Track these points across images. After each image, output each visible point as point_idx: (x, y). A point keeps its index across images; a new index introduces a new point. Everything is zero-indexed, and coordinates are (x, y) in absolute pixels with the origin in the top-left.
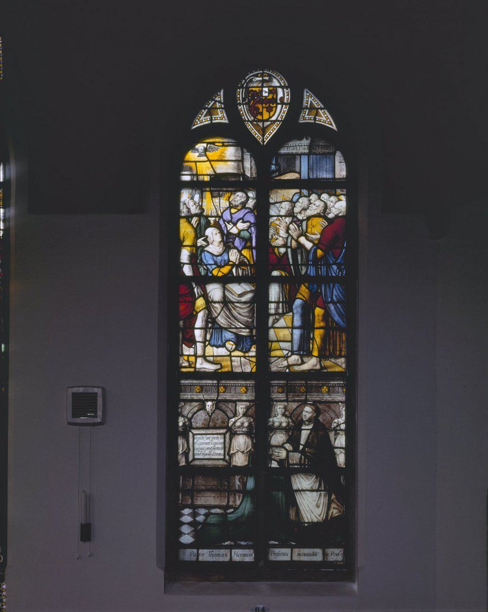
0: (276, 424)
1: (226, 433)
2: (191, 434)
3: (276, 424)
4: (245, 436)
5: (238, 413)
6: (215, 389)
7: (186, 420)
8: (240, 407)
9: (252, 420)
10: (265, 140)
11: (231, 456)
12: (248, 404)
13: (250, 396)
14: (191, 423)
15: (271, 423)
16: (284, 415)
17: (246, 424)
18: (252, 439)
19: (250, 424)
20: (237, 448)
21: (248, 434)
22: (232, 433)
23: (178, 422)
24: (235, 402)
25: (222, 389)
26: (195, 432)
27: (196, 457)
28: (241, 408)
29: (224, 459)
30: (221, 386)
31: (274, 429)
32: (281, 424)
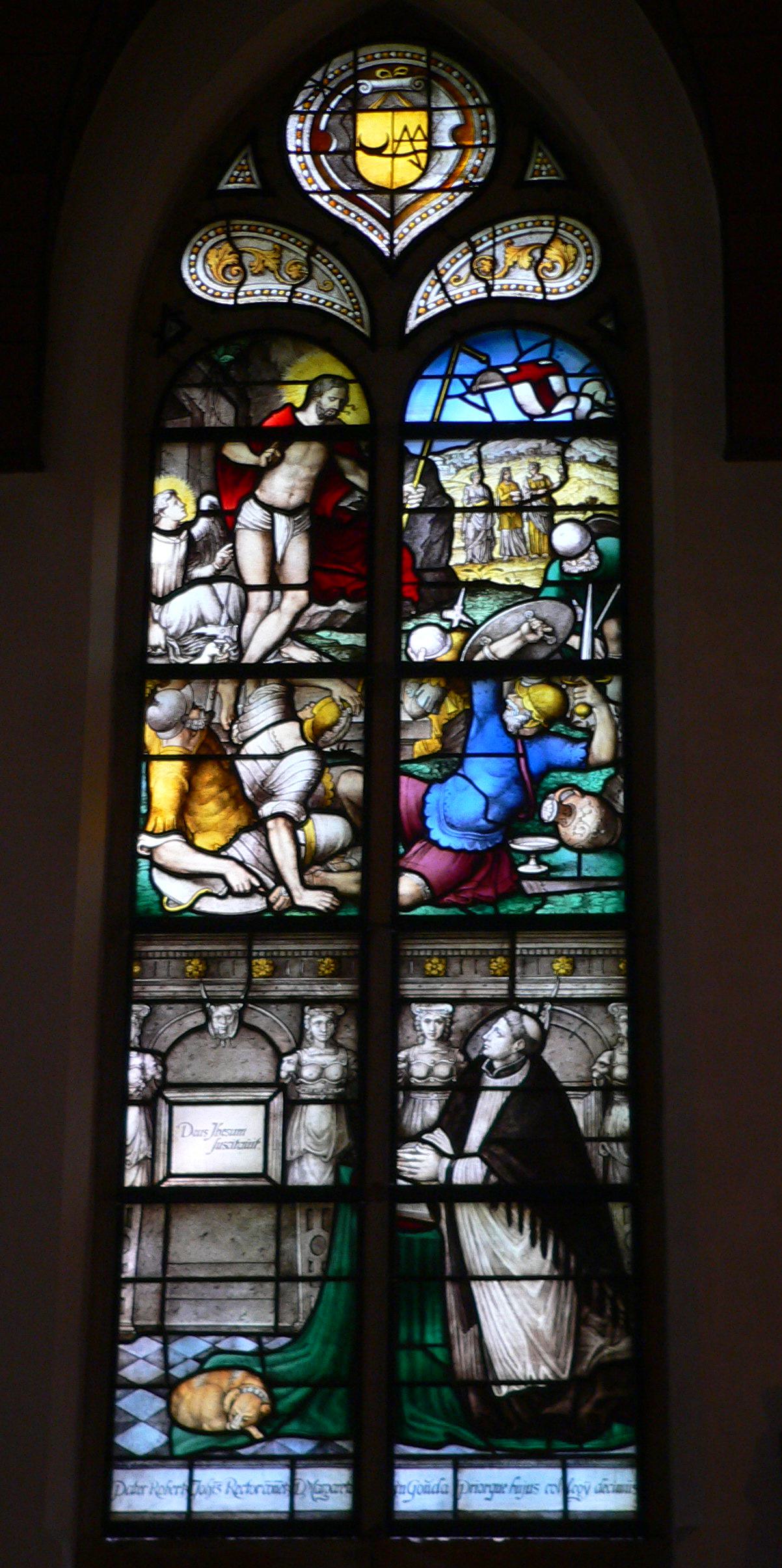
2: (163, 1108)
8: (314, 1020)
10: (396, 241)
11: (286, 1165)
17: (334, 1072)
22: (293, 1105)
28: (319, 1023)
30: (258, 957)
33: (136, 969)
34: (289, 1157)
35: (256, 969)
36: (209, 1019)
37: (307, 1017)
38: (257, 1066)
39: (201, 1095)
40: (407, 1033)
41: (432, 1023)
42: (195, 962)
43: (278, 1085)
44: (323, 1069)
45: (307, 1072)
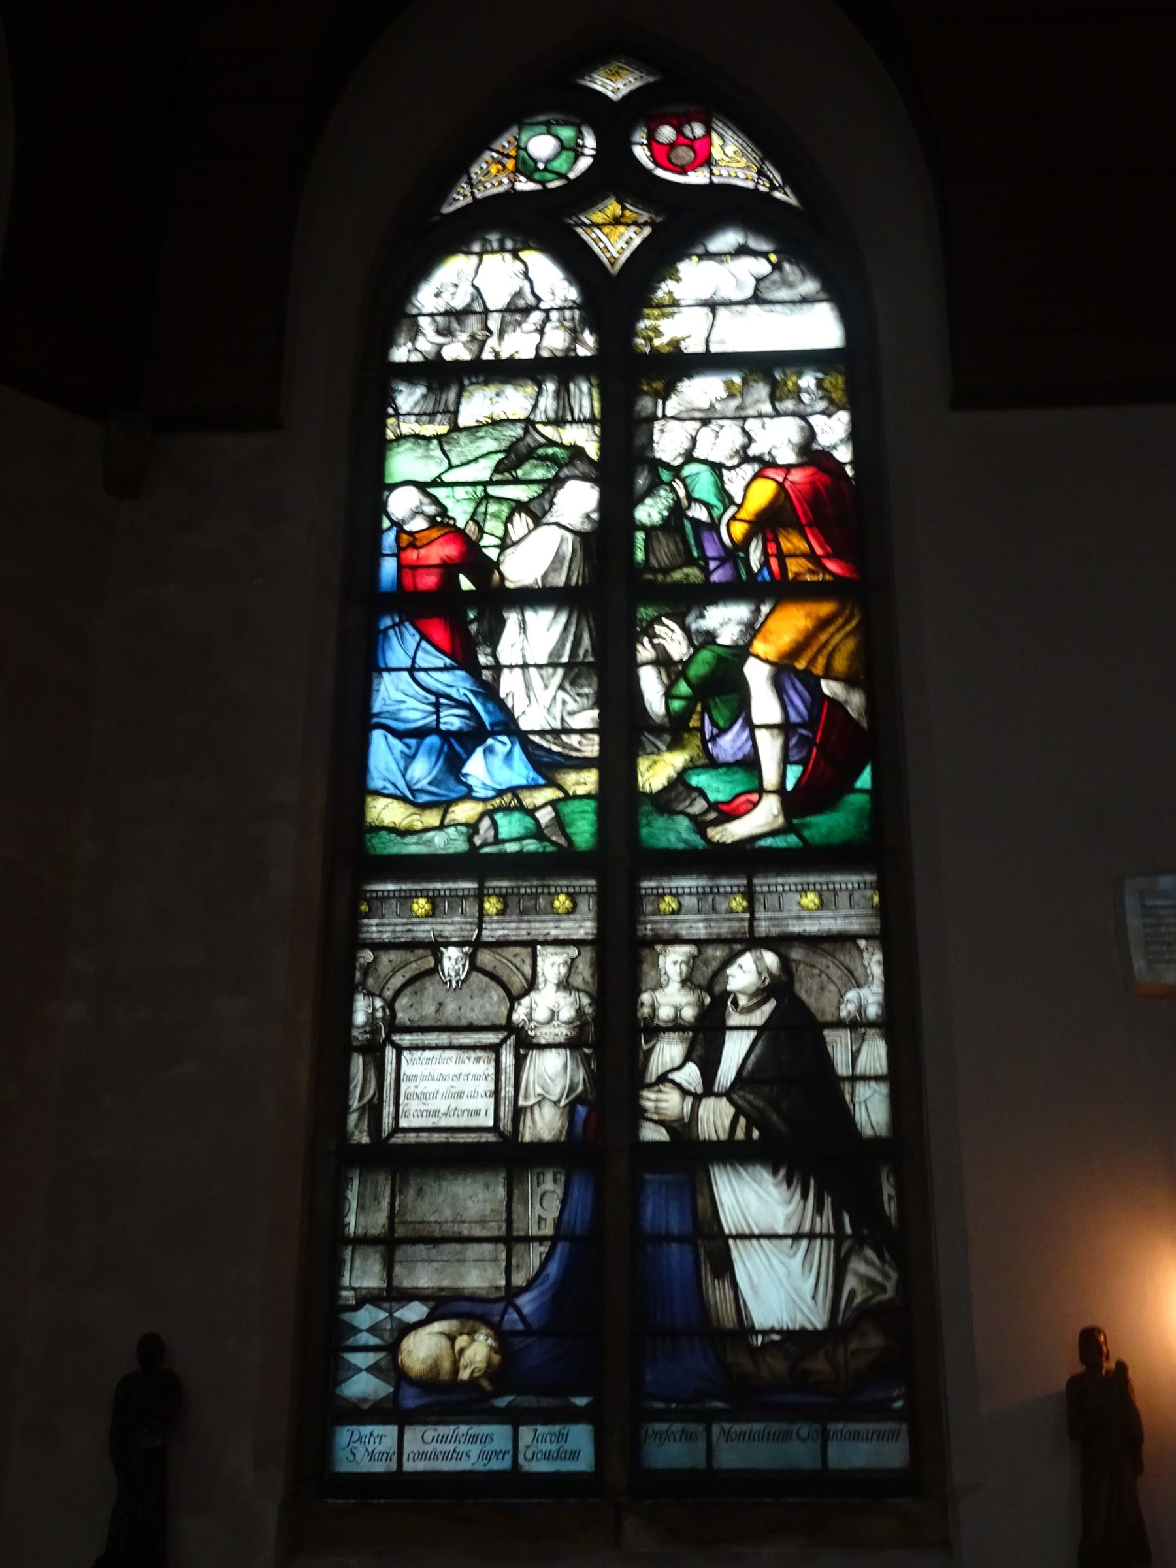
0: (665, 1013)
1: (504, 1041)
3: (665, 1013)
4: (562, 1051)
5: (541, 979)
6: (471, 908)
7: (379, 1003)
9: (586, 1001)
11: (518, 1113)
12: (573, 951)
13: (585, 927)
14: (393, 1014)
15: (646, 1011)
16: (687, 982)
17: (567, 1013)
18: (586, 1059)
19: (580, 1012)
20: (539, 1090)
21: (570, 1044)
23: (350, 1011)
24: (532, 945)
25: (492, 906)
26: (406, 1039)
27: (403, 1123)
29: (495, 1129)
30: (489, 895)
31: (654, 1030)
32: (678, 1009)
33: (364, 908)
34: (521, 1102)
35: (487, 906)
36: (439, 961)
37: (539, 959)
38: (491, 1005)
39: (431, 1038)
40: (649, 978)
41: (678, 965)
42: (422, 901)
43: (510, 1028)
44: (553, 1012)
45: (541, 1014)
